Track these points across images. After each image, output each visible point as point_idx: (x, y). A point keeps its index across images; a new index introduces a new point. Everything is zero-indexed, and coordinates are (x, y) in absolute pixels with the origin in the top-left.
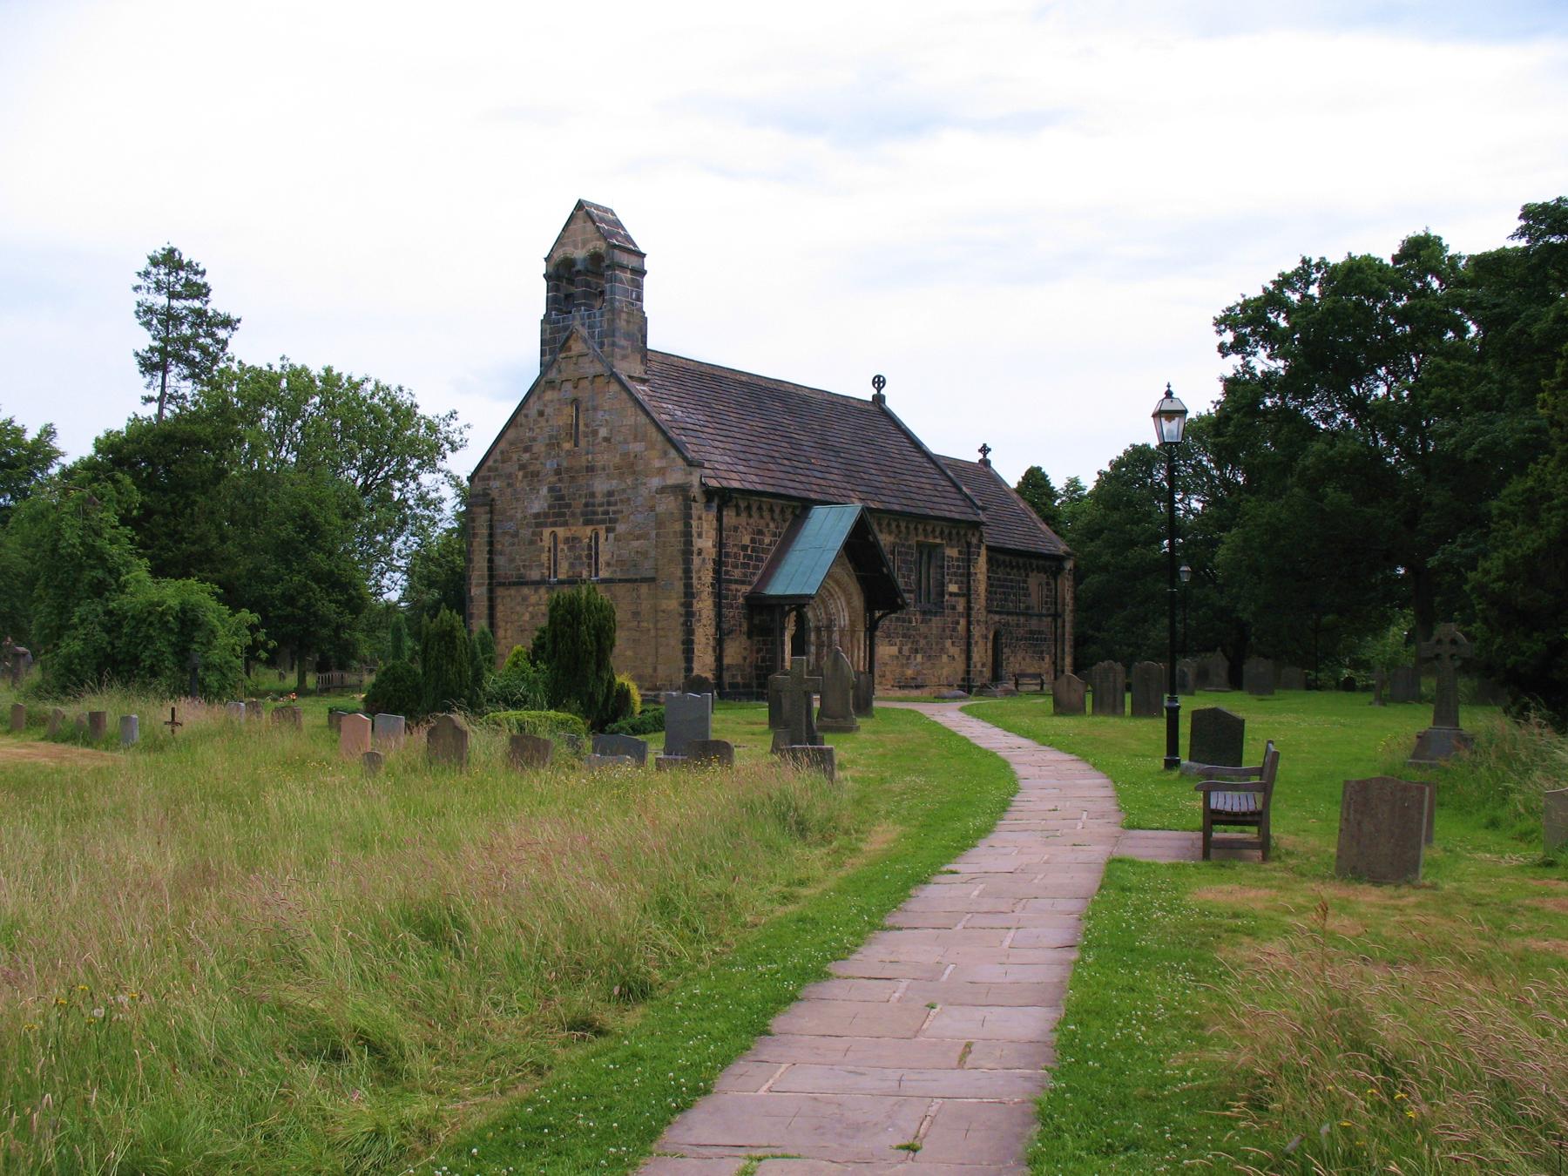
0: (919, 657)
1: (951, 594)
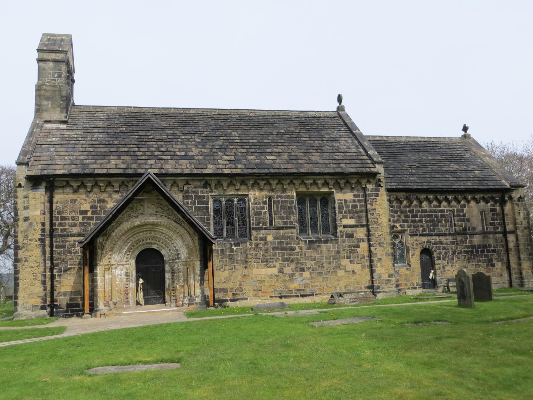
0: (306, 274)
1: (345, 227)
